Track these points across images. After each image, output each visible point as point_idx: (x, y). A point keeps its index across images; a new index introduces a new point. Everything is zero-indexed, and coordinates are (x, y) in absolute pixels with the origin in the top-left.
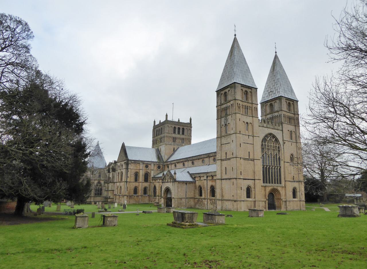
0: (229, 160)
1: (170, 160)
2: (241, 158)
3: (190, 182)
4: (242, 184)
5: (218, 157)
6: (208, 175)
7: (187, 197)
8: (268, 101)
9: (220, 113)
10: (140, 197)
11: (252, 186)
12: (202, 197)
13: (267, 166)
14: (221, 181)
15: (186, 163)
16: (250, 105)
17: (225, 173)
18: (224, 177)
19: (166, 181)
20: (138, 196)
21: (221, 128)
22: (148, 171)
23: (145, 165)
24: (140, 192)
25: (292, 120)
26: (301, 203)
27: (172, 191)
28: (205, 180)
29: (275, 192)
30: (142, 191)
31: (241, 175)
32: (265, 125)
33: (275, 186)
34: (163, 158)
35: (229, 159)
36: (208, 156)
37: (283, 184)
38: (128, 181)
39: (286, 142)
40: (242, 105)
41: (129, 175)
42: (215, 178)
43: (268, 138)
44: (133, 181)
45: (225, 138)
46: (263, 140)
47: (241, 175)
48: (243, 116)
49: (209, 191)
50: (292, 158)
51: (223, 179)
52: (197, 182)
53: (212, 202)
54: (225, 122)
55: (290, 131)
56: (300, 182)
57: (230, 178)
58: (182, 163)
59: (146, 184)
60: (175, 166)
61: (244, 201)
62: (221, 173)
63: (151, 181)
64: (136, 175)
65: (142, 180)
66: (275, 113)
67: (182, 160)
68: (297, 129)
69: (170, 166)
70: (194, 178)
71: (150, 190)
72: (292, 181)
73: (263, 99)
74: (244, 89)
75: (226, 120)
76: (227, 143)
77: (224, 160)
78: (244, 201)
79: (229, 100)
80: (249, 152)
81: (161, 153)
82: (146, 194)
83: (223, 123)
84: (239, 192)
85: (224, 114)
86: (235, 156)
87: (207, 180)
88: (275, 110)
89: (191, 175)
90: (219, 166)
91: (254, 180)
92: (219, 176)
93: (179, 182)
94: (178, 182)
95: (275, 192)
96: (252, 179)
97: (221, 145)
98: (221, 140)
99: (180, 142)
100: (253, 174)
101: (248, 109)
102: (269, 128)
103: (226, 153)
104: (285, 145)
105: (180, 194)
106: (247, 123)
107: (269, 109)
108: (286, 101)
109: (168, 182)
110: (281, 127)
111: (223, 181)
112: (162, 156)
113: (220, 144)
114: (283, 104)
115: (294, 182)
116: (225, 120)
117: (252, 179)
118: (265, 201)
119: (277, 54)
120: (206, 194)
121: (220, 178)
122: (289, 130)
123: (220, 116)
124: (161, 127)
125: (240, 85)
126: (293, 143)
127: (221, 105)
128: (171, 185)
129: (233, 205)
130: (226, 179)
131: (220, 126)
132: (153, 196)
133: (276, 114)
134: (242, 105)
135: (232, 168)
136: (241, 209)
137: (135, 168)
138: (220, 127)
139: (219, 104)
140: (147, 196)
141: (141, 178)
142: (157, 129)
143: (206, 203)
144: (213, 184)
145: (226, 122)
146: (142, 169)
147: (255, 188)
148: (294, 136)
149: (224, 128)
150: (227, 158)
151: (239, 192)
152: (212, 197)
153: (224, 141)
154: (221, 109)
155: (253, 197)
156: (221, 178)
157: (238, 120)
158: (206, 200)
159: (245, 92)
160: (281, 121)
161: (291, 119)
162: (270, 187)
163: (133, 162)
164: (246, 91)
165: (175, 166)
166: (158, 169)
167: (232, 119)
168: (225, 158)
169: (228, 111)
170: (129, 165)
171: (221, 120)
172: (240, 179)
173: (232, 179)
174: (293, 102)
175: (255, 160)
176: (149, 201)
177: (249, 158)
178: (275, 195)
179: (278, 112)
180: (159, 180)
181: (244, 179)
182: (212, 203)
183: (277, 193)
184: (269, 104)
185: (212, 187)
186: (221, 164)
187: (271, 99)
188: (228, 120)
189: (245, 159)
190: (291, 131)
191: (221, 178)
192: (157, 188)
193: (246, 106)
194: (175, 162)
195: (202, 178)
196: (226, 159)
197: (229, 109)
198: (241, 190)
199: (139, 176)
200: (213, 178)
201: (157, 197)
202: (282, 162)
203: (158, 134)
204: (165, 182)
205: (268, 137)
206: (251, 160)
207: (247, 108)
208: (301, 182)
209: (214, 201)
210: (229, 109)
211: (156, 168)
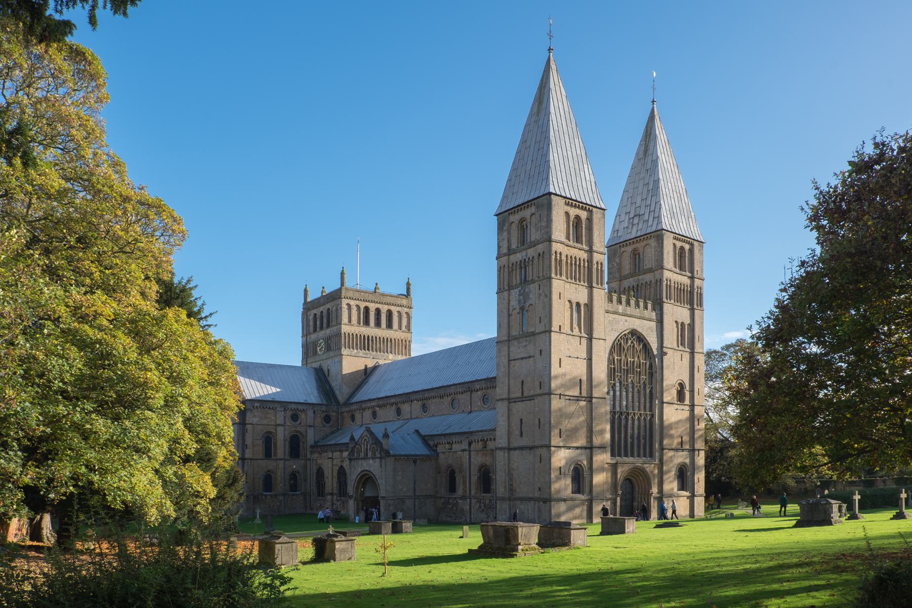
0: (530, 400)
1: (355, 400)
3: (425, 458)
5: (501, 391)
6: (472, 438)
7: (417, 494)
8: (628, 242)
9: (506, 274)
10: (281, 498)
12: (456, 495)
13: (621, 413)
14: (509, 454)
15: (405, 408)
17: (517, 432)
18: (515, 444)
19: (362, 455)
20: (276, 496)
21: (509, 315)
22: (298, 429)
23: (289, 413)
24: (280, 484)
27: (381, 482)
28: (464, 450)
29: (638, 476)
30: (285, 481)
32: (621, 308)
34: (337, 392)
35: (531, 398)
36: (468, 387)
38: (247, 456)
39: (670, 352)
40: (567, 256)
41: (249, 441)
42: (491, 445)
43: (627, 342)
44: (261, 458)
45: (519, 343)
46: (613, 347)
49: (474, 479)
51: (515, 449)
52: (442, 456)
53: (482, 505)
54: (519, 301)
55: (680, 321)
57: (530, 444)
58: (394, 407)
59: (295, 465)
60: (374, 415)
62: (509, 433)
63: (309, 456)
64: (268, 441)
65: (285, 455)
66: (644, 273)
67: (393, 400)
68: (696, 317)
69: (358, 416)
70: (433, 448)
71: (306, 480)
73: (615, 235)
75: (525, 296)
76: (526, 358)
77: (517, 400)
79: (533, 239)
81: (328, 378)
82: (296, 491)
83: (514, 303)
85: (516, 280)
86: (547, 391)
87: (470, 452)
88: (645, 268)
89: (425, 439)
90: (502, 416)
92: (502, 442)
93: (397, 457)
94: (393, 459)
95: (638, 476)
97: (509, 361)
98: (509, 347)
99: (380, 348)
102: (631, 316)
103: (523, 381)
104: (665, 358)
105: (400, 488)
107: (630, 263)
109: (366, 458)
110: (659, 312)
111: (512, 452)
112: (335, 389)
113: (507, 360)
114: (665, 252)
116: (520, 295)
120: (468, 484)
121: (505, 445)
122: (676, 322)
123: (506, 283)
124: (328, 306)
127: (510, 252)
128: (376, 464)
129: (540, 510)
130: (522, 448)
131: (505, 311)
132: (317, 495)
133: (648, 277)
134: (567, 256)
135: (537, 422)
137: (265, 422)
138: (506, 315)
139: (505, 251)
140: (298, 494)
141: (281, 448)
142: (315, 311)
143: (468, 508)
144: (488, 460)
145: (525, 303)
146: (282, 425)
149: (516, 319)
150: (525, 395)
152: (484, 493)
153: (517, 350)
154: (510, 265)
155: (587, 489)
156: (509, 446)
157: (555, 296)
158: (468, 500)
160: (658, 297)
162: (628, 463)
163: (256, 405)
165: (374, 415)
166: (324, 423)
167: (540, 295)
168: (519, 395)
169: (529, 269)
171: (509, 296)
173: (537, 447)
176: (306, 507)
179: (651, 270)
180: (333, 452)
182: (483, 508)
184: (629, 249)
185: (483, 469)
186: (509, 410)
187: (636, 238)
188: (528, 295)
191: (509, 446)
192: (328, 473)
193: (575, 258)
194: (373, 404)
195: (456, 447)
196: (523, 399)
197: (531, 266)
199: (275, 444)
200: (485, 447)
201: (329, 497)
203: (318, 326)
204: (359, 459)
205: (627, 339)
209: (487, 502)
210: (531, 266)
211: (319, 420)
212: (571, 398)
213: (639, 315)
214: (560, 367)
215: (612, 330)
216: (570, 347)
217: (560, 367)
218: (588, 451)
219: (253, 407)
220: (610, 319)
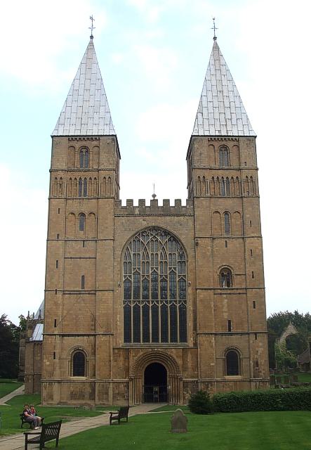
4: (58, 346)
11: (88, 350)
16: (95, 174)
31: (55, 326)
33: (160, 346)
37: (190, 342)
47: (55, 326)
50: (226, 275)
55: (222, 212)
56: (253, 337)
61: (59, 382)
72: (225, 334)
74: (78, 145)
80: (83, 277)
84: (48, 363)
91: (95, 335)
96: (88, 335)
101: (85, 184)
104: (199, 249)
106: (82, 214)
115: (232, 334)
117: (88, 335)
118: (128, 383)
119: (217, 41)
136: (52, 399)
147: (94, 353)
148: (235, 221)
151: (48, 363)
159: (84, 150)
162: (142, 348)
164: (85, 147)
177: (83, 287)
181: (63, 336)
190: (226, 213)
202: (189, 290)
206: (89, 294)
207: (82, 183)
208: (256, 334)
216: (71, 250)
218: (92, 338)
220: (124, 221)
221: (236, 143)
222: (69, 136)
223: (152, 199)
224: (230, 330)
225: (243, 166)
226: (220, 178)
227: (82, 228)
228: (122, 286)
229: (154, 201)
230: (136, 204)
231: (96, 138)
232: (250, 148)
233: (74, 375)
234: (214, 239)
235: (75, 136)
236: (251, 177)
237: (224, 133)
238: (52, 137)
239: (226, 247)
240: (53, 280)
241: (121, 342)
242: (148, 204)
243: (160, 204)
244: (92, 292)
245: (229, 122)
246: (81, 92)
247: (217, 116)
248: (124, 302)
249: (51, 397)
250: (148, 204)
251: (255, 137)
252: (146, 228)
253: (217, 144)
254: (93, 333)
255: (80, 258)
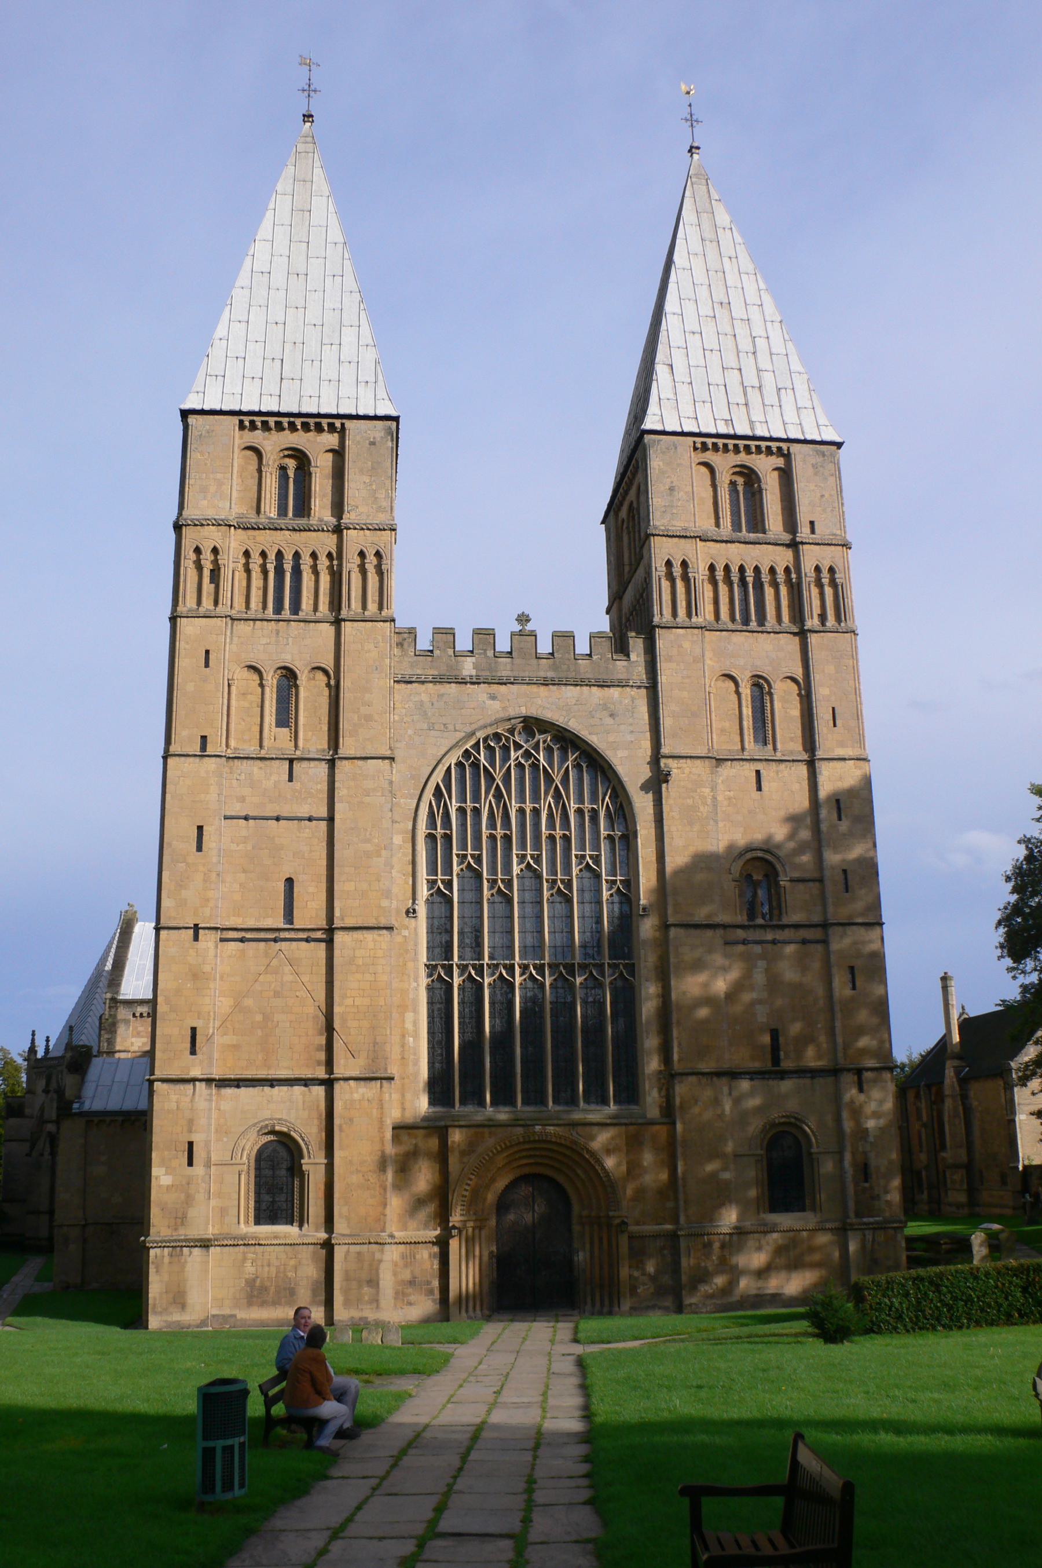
2: (196, 928)
25: (769, 592)
26: (853, 1247)
31: (193, 1052)
37: (652, 1097)
47: (193, 1052)
48: (242, 627)
61: (205, 1244)
74: (273, 444)
78: (205, 1244)
80: (290, 881)
96: (306, 1082)
100: (322, 1040)
104: (670, 793)
108: (706, 465)
115: (782, 1075)
117: (306, 1082)
125: (235, 420)
126: (768, 772)
136: (183, 1306)
161: (759, 586)
170: (121, 1030)
172: (181, 1087)
174: (787, 457)
175: (339, 937)
178: (570, 1191)
181: (223, 1083)
183: (579, 1172)
189: (244, 935)
198: (190, 1163)
205: (506, 749)
212: (249, 935)
213: (550, 674)
214: (199, 848)
215: (431, 728)
216: (246, 791)
217: (199, 848)
219: (134, 1015)
220: (424, 697)
221: (780, 462)
222: (240, 413)
223: (517, 628)
224: (776, 1060)
225: (804, 533)
226: (735, 569)
227: (286, 717)
228: (422, 910)
229: (524, 635)
230: (464, 643)
231: (331, 426)
232: (826, 479)
233: (258, 1222)
234: (720, 761)
235: (260, 413)
236: (832, 570)
237: (743, 429)
238: (185, 414)
239: (759, 788)
240: (184, 893)
241: (422, 1104)
242: (503, 644)
243: (544, 646)
244: (319, 935)
245: (754, 396)
246: (279, 278)
247: (716, 377)
248: (431, 969)
249: (179, 1300)
250: (503, 644)
251: (839, 445)
252: (497, 722)
253: (725, 463)
254: (321, 1073)
255: (278, 819)
